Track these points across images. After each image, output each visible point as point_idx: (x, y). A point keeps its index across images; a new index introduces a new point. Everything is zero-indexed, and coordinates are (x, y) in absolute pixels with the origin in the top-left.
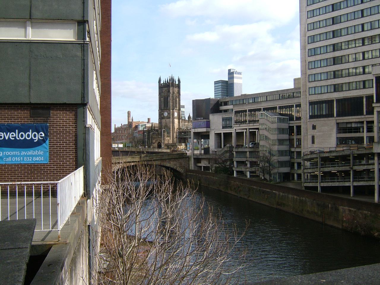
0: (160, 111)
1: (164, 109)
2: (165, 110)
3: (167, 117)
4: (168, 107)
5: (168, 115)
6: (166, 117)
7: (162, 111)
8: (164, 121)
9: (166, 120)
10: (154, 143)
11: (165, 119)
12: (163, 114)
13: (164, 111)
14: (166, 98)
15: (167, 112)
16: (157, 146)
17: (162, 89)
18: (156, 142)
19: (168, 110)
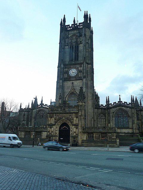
0: (62, 66)
1: (71, 65)
2: (72, 66)
3: (75, 77)
4: (78, 60)
5: (77, 74)
6: (73, 77)
7: (66, 68)
8: (68, 84)
9: (73, 83)
10: (51, 126)
11: (72, 82)
12: (67, 73)
13: (71, 68)
14: (74, 47)
15: (77, 69)
16: (58, 132)
17: (67, 32)
18: (56, 122)
19: (77, 66)
